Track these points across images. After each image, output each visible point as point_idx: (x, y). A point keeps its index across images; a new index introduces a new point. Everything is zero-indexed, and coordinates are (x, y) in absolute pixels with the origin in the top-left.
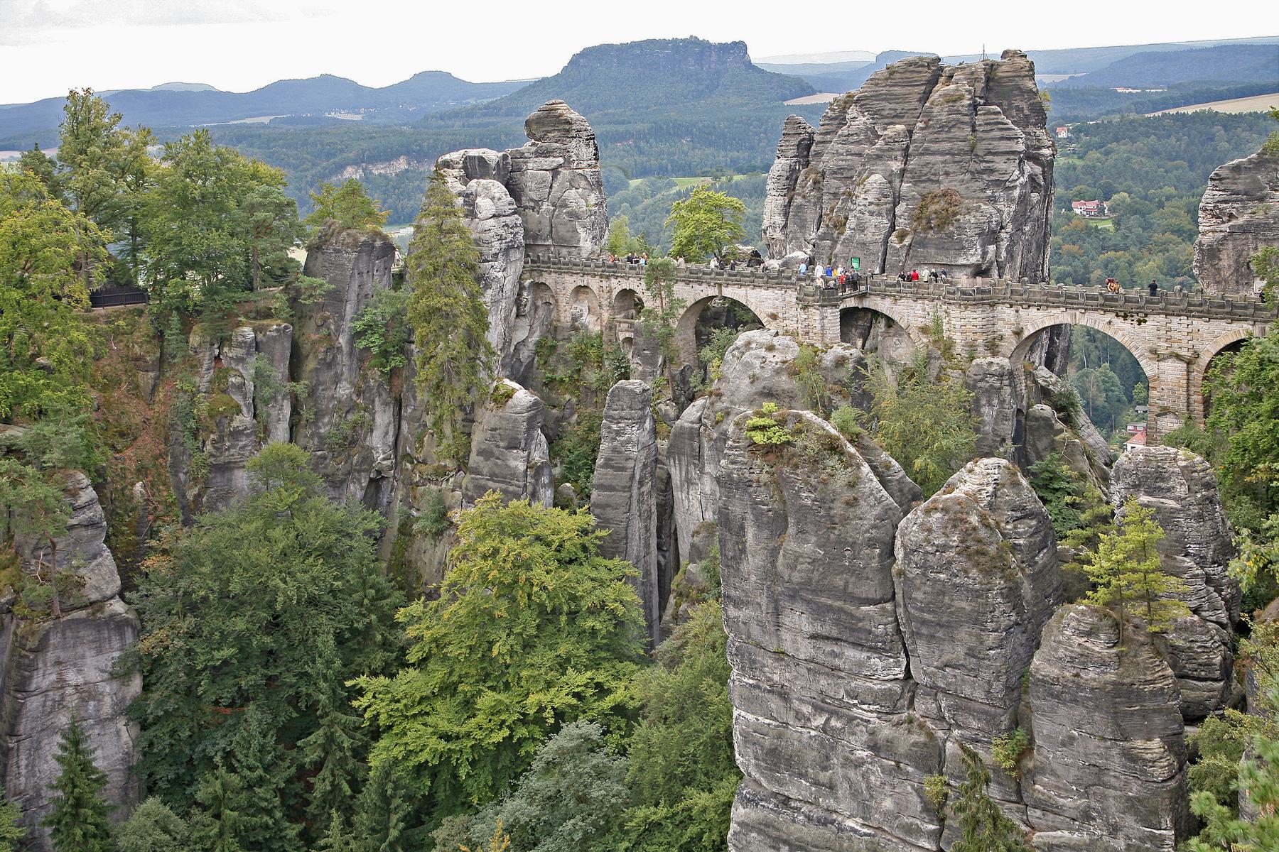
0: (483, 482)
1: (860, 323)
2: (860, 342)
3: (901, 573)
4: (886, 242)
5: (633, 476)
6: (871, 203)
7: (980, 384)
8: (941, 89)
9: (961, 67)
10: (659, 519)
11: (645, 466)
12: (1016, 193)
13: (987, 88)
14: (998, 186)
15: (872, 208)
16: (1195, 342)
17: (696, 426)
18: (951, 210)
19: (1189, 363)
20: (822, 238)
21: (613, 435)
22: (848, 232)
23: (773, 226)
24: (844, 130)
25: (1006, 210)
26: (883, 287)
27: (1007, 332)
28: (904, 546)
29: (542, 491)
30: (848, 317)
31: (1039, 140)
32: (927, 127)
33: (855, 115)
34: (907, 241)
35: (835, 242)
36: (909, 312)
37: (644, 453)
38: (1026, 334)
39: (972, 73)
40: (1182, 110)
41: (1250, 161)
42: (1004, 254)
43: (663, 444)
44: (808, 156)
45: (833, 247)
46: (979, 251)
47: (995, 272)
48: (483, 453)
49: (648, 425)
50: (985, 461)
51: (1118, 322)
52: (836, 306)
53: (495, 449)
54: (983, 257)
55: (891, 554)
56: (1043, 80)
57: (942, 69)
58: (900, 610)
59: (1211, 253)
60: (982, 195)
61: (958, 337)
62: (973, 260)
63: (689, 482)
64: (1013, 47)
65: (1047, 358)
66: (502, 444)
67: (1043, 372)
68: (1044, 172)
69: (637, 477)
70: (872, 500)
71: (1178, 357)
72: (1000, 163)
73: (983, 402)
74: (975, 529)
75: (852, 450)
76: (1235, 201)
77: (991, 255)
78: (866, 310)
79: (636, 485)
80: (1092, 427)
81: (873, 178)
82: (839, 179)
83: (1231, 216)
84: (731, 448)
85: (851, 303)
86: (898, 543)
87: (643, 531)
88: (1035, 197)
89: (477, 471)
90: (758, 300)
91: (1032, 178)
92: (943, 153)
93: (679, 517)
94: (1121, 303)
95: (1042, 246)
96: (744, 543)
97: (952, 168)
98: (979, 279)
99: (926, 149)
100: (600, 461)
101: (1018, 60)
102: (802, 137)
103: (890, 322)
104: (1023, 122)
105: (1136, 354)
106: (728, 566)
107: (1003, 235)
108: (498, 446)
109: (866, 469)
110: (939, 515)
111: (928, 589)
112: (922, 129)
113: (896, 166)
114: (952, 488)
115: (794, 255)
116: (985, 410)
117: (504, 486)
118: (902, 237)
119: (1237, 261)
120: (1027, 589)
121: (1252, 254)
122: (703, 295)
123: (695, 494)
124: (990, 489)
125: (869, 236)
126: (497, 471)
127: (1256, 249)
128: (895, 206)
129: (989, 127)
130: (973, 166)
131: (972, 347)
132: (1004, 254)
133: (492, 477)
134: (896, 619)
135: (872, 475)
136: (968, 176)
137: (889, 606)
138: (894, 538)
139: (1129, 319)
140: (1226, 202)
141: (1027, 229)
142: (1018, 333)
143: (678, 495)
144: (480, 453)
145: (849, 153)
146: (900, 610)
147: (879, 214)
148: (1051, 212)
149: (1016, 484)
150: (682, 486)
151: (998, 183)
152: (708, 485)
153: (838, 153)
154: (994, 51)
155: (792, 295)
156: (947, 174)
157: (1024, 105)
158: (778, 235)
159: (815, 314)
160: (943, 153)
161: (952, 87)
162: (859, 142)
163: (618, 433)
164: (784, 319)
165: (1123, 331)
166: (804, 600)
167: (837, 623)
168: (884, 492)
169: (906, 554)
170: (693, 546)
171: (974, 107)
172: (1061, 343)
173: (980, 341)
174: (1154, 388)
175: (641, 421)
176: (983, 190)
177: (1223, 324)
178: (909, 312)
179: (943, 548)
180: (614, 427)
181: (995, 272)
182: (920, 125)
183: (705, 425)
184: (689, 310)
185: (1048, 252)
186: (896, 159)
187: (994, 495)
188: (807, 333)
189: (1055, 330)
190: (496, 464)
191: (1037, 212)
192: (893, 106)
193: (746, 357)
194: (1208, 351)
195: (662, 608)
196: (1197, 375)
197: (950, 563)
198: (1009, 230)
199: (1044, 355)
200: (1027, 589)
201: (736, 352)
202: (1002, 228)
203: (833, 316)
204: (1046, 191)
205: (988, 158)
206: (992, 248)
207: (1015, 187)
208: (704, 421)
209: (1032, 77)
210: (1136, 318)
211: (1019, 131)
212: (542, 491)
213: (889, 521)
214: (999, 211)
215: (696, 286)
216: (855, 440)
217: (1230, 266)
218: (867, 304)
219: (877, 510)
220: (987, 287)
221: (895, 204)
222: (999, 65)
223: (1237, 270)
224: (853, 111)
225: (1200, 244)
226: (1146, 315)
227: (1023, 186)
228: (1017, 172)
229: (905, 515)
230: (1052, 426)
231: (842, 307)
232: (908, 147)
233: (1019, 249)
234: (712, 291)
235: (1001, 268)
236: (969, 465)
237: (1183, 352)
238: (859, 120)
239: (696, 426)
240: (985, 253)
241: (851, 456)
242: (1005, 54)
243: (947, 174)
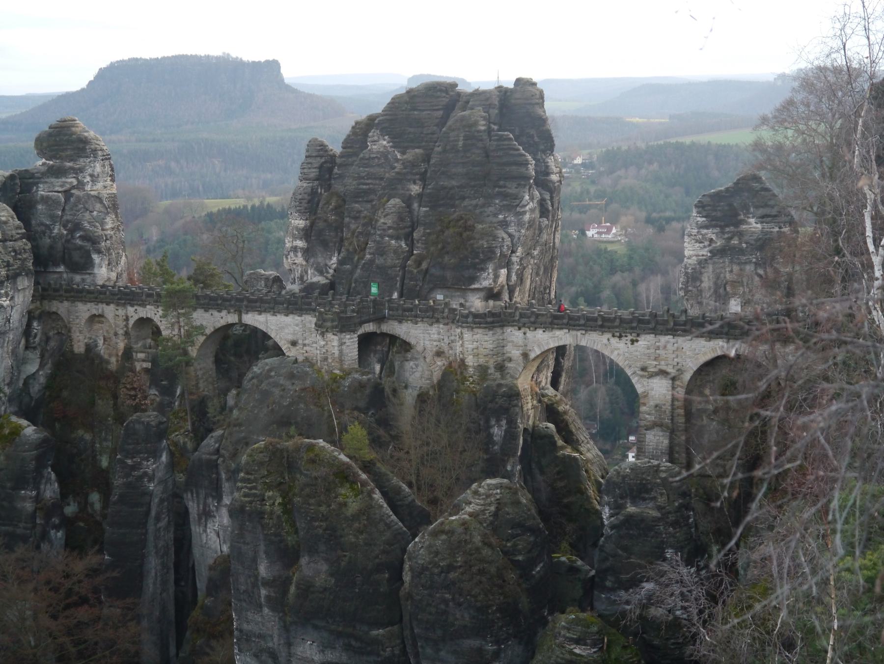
1: (379, 348)
2: (378, 368)
3: (409, 596)
4: (403, 267)
5: (148, 513)
6: (390, 228)
7: (490, 405)
8: (458, 114)
9: (477, 94)
10: (177, 553)
11: (162, 501)
12: (527, 217)
13: (501, 114)
14: (509, 210)
16: (679, 360)
17: (214, 457)
18: (465, 235)
19: (673, 379)
20: (341, 263)
22: (368, 256)
23: (295, 249)
24: (364, 154)
25: (517, 234)
26: (400, 312)
27: (516, 353)
28: (411, 569)
29: (53, 532)
30: (366, 342)
31: (547, 167)
32: (445, 151)
33: (376, 138)
34: (424, 265)
35: (356, 267)
36: (422, 335)
37: (160, 488)
38: (532, 356)
39: (487, 100)
40: (681, 140)
41: (727, 189)
42: (514, 277)
43: (181, 478)
44: (330, 179)
45: (352, 272)
46: (491, 276)
47: (506, 296)
49: (164, 458)
50: (489, 481)
51: (614, 341)
52: (354, 332)
54: (495, 281)
55: (400, 579)
56: (551, 107)
57: (459, 94)
58: (407, 633)
59: (694, 277)
60: (495, 220)
61: (470, 361)
62: (486, 283)
63: (206, 515)
64: (525, 75)
65: (553, 378)
67: (551, 391)
68: (552, 198)
69: (153, 513)
70: (381, 526)
71: (663, 373)
72: (512, 188)
73: (493, 422)
74: (478, 549)
75: (364, 476)
76: (715, 226)
77: (502, 279)
78: (384, 335)
79: (151, 521)
80: (592, 443)
81: (392, 202)
83: (711, 240)
84: (243, 480)
85: (370, 328)
86: (407, 566)
87: (159, 568)
88: (545, 221)
90: (281, 327)
91: (542, 203)
93: (196, 552)
94: (617, 323)
95: (548, 270)
96: (256, 577)
98: (491, 303)
100: (114, 498)
101: (530, 88)
102: (323, 160)
103: (406, 346)
104: (532, 148)
105: (629, 372)
106: (240, 600)
107: (514, 259)
109: (377, 495)
110: (444, 537)
111: (433, 610)
112: (440, 153)
113: (415, 189)
114: (457, 509)
115: (315, 279)
116: (496, 430)
117: (10, 529)
118: (419, 263)
119: (716, 283)
120: (525, 603)
121: (728, 276)
122: (222, 323)
123: (213, 526)
124: (493, 508)
125: (390, 260)
127: (731, 271)
128: (413, 230)
129: (500, 153)
131: (483, 370)
132: (514, 277)
134: (403, 642)
135: (382, 501)
136: (482, 201)
137: (396, 628)
138: (402, 562)
139: (624, 339)
140: (707, 227)
141: (536, 253)
142: (525, 355)
143: (195, 529)
145: (370, 176)
146: (407, 633)
147: (397, 238)
148: (558, 236)
149: (517, 503)
150: (200, 519)
151: (509, 208)
152: (223, 518)
154: (508, 81)
155: (310, 320)
157: (532, 132)
158: (300, 260)
159: (333, 340)
161: (467, 113)
163: (134, 468)
164: (304, 345)
165: (617, 349)
166: (316, 627)
167: (348, 648)
168: (394, 517)
169: (412, 577)
170: (210, 580)
171: (489, 131)
172: (567, 363)
173: (491, 364)
174: (644, 404)
175: (155, 454)
176: (495, 215)
177: (702, 342)
178: (422, 335)
179: (451, 568)
180: (129, 462)
181: (506, 296)
182: (439, 149)
183: (223, 456)
184: (209, 337)
185: (555, 275)
186: (415, 183)
187: (495, 515)
188: (326, 359)
189: (561, 351)
191: (545, 236)
192: (412, 130)
193: (264, 386)
194: (691, 366)
195: (179, 646)
196: (681, 393)
197: (453, 583)
198: (518, 254)
199: (550, 375)
200: (525, 603)
201: (255, 381)
202: (513, 252)
203: (351, 342)
204: (553, 217)
205: (502, 183)
206: (504, 272)
207: (524, 213)
208: (222, 451)
209: (542, 105)
210: (630, 337)
211: (529, 158)
212: (53, 532)
213: (400, 543)
214: (510, 235)
215: (216, 313)
216: (367, 467)
217: (710, 288)
218: (386, 328)
219: (388, 535)
220: (497, 310)
221: (413, 228)
222: (511, 90)
223: (716, 292)
224: (373, 134)
225: (686, 268)
226: (638, 335)
227: (532, 211)
228: (527, 197)
229: (414, 539)
230: (554, 443)
231: (361, 331)
232: (426, 171)
233: (528, 273)
234: (232, 318)
235: (511, 292)
236: (474, 486)
237: (670, 369)
238: (380, 144)
239: (214, 457)
240: (496, 277)
241: (364, 484)
242: (519, 81)
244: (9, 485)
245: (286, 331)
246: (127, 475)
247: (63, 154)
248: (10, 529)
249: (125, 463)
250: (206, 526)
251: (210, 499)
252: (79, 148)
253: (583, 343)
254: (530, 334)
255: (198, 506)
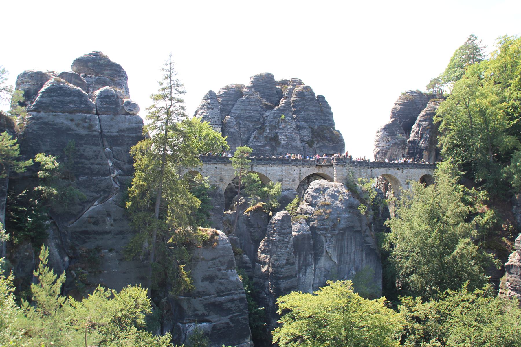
0: (213, 300)
6: (294, 129)
15: (295, 131)
21: (285, 245)
48: (211, 279)
53: (219, 274)
66: (222, 268)
82: (249, 122)
89: (204, 294)
92: (313, 111)
97: (318, 117)
99: (307, 108)
108: (220, 270)
117: (230, 297)
126: (222, 288)
130: (323, 117)
133: (219, 294)
144: (204, 279)
153: (246, 110)
156: (316, 119)
160: (313, 111)
162: (255, 105)
190: (221, 284)
243: (316, 119)
244: (225, 267)
245: (276, 174)
246: (287, 247)
247: (106, 72)
248: (230, 297)
249: (283, 240)
250: (305, 272)
251: (310, 256)
252: (116, 70)
253: (389, 173)
254: (373, 170)
255: (299, 263)
